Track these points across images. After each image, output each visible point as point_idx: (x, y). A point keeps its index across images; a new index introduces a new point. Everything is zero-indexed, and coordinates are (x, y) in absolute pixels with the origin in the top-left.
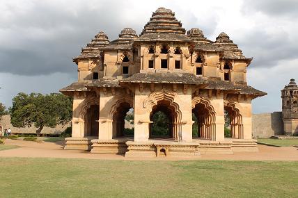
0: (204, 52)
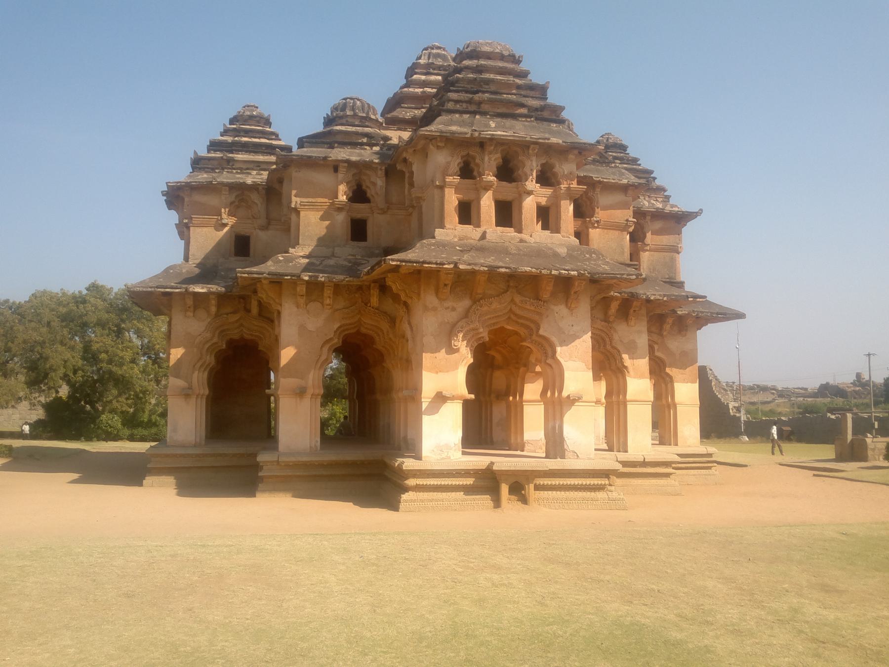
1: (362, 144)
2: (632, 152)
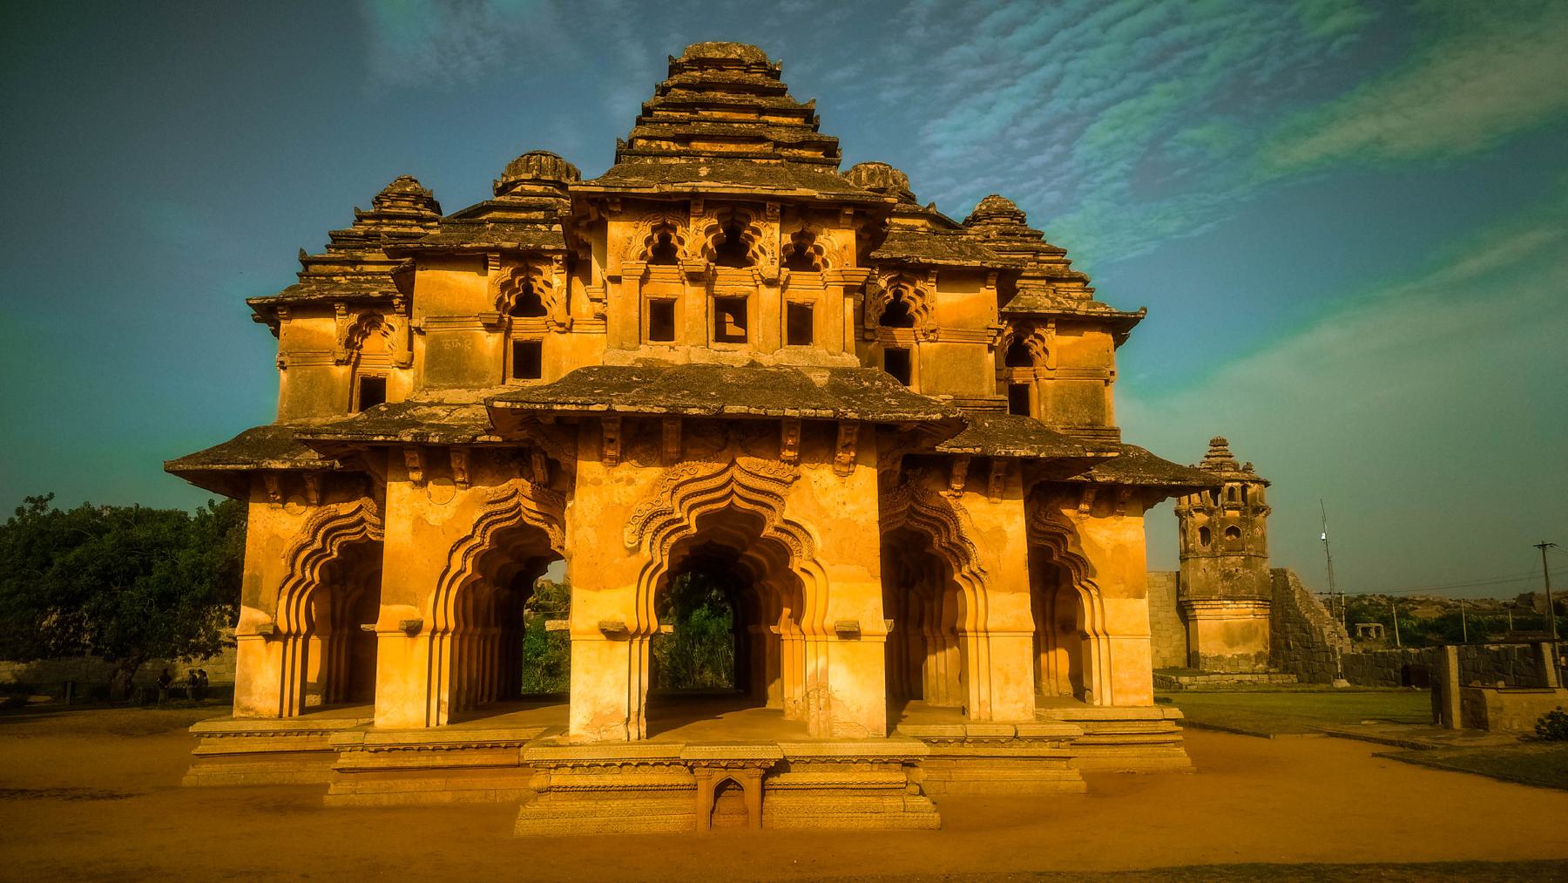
1: (534, 222)
2: (1032, 224)
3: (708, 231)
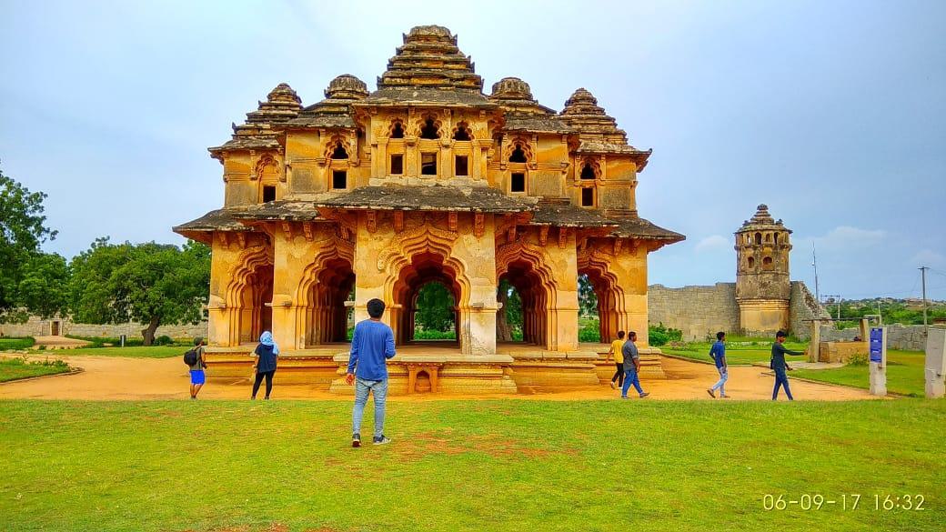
0: (530, 135)
3: (417, 122)
